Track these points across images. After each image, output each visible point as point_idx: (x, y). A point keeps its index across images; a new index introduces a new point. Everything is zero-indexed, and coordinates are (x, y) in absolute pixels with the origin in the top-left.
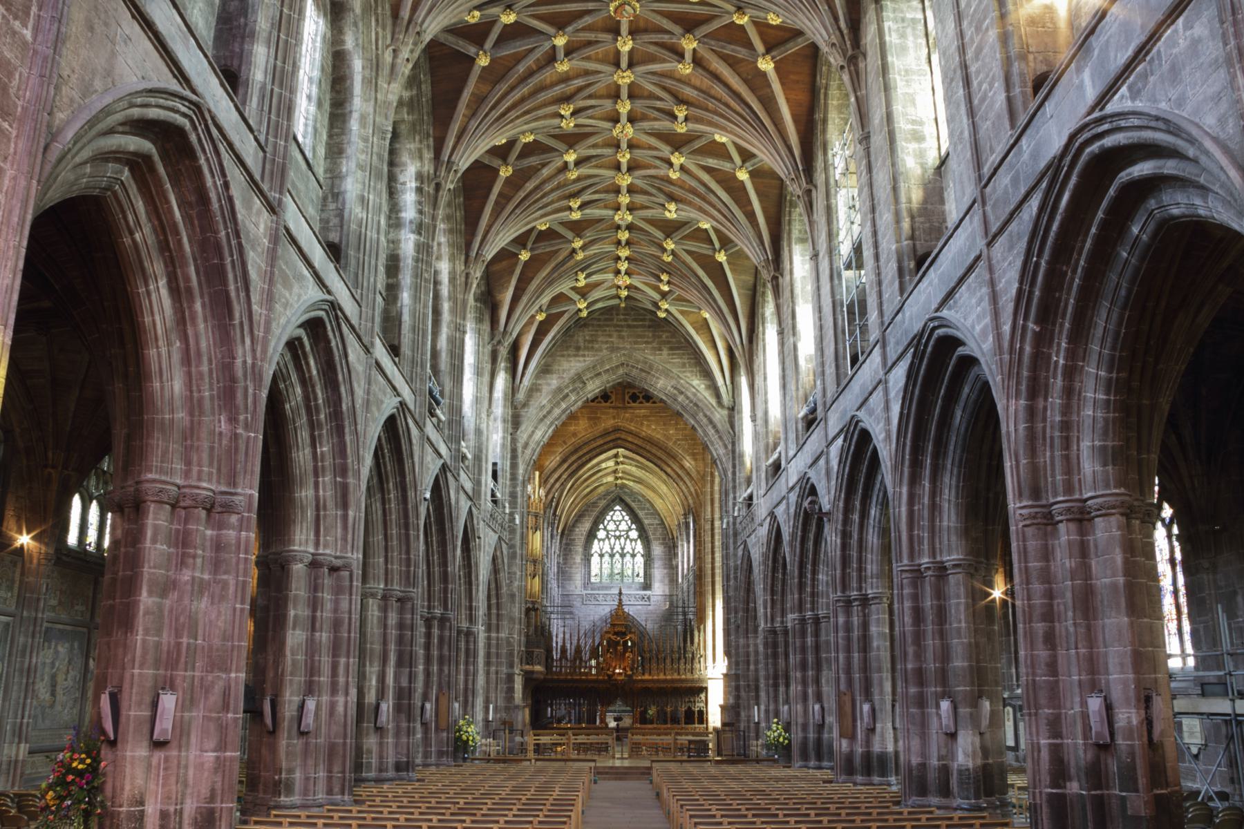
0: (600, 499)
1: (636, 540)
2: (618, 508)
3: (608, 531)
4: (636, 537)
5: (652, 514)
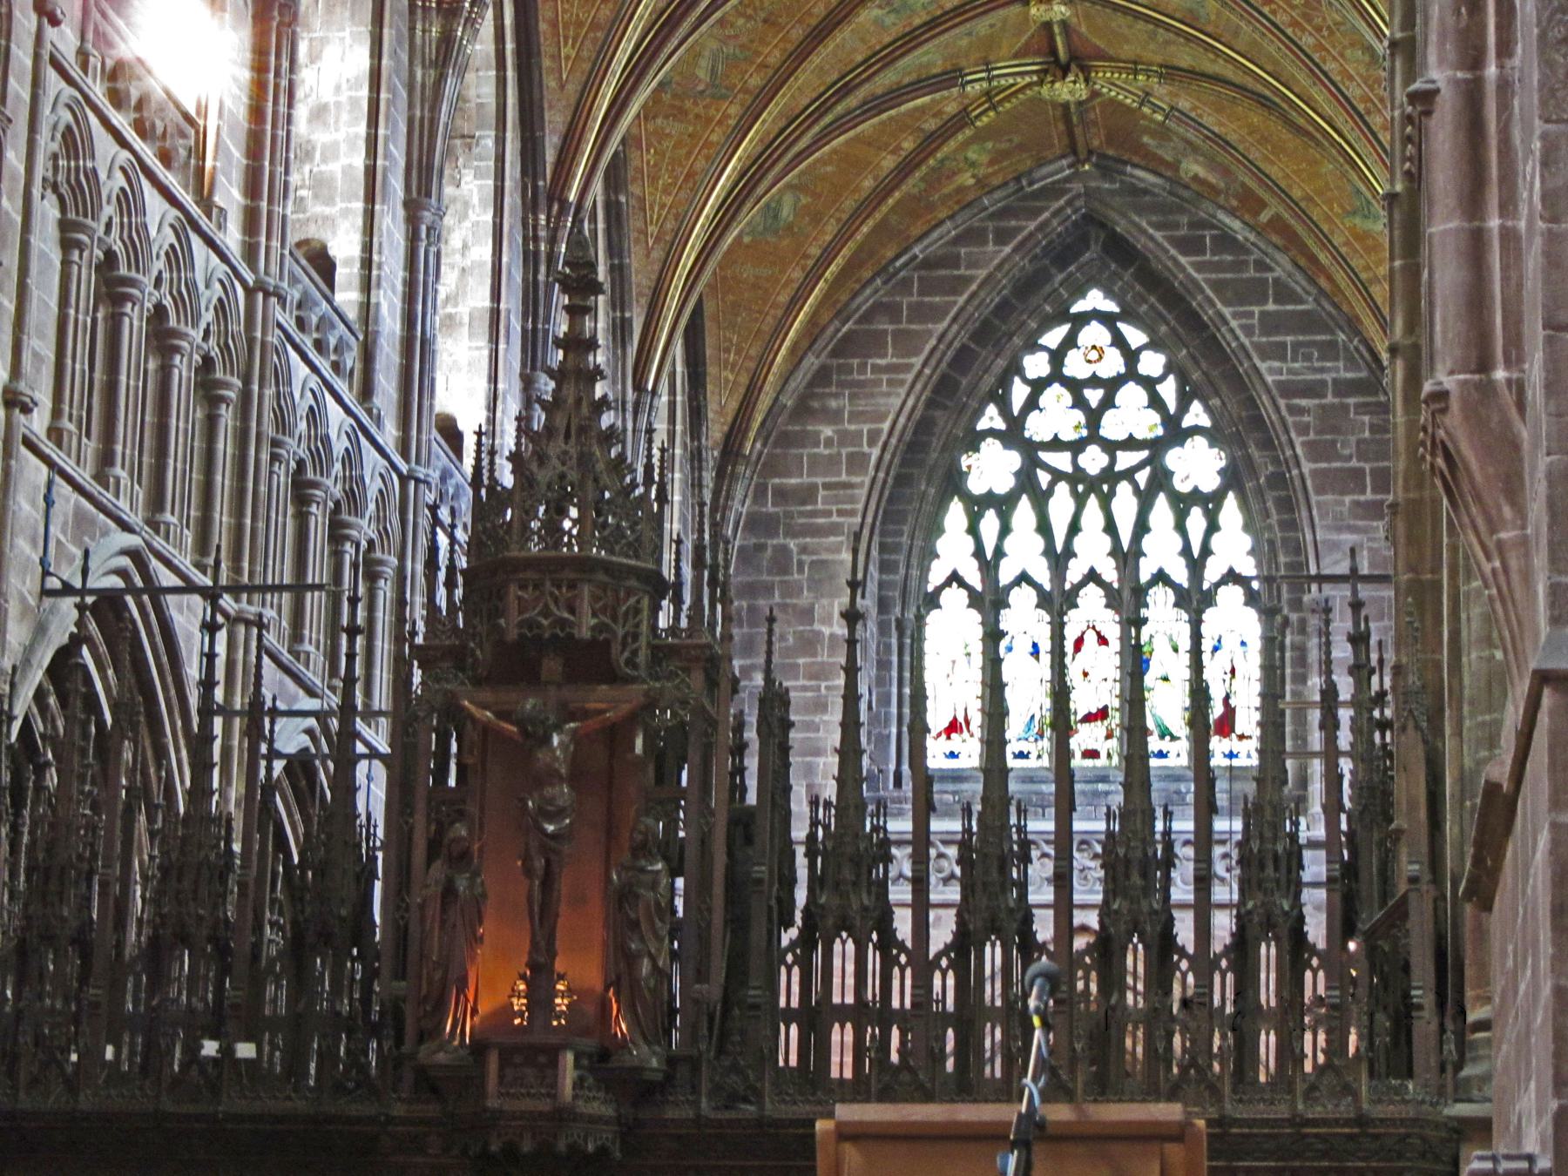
0: (972, 236)
1: (1211, 503)
2: (1095, 300)
3: (1031, 451)
4: (1210, 483)
5: (1307, 323)
